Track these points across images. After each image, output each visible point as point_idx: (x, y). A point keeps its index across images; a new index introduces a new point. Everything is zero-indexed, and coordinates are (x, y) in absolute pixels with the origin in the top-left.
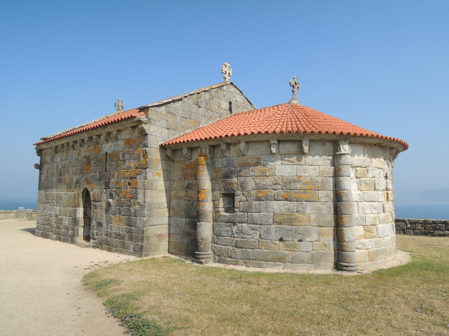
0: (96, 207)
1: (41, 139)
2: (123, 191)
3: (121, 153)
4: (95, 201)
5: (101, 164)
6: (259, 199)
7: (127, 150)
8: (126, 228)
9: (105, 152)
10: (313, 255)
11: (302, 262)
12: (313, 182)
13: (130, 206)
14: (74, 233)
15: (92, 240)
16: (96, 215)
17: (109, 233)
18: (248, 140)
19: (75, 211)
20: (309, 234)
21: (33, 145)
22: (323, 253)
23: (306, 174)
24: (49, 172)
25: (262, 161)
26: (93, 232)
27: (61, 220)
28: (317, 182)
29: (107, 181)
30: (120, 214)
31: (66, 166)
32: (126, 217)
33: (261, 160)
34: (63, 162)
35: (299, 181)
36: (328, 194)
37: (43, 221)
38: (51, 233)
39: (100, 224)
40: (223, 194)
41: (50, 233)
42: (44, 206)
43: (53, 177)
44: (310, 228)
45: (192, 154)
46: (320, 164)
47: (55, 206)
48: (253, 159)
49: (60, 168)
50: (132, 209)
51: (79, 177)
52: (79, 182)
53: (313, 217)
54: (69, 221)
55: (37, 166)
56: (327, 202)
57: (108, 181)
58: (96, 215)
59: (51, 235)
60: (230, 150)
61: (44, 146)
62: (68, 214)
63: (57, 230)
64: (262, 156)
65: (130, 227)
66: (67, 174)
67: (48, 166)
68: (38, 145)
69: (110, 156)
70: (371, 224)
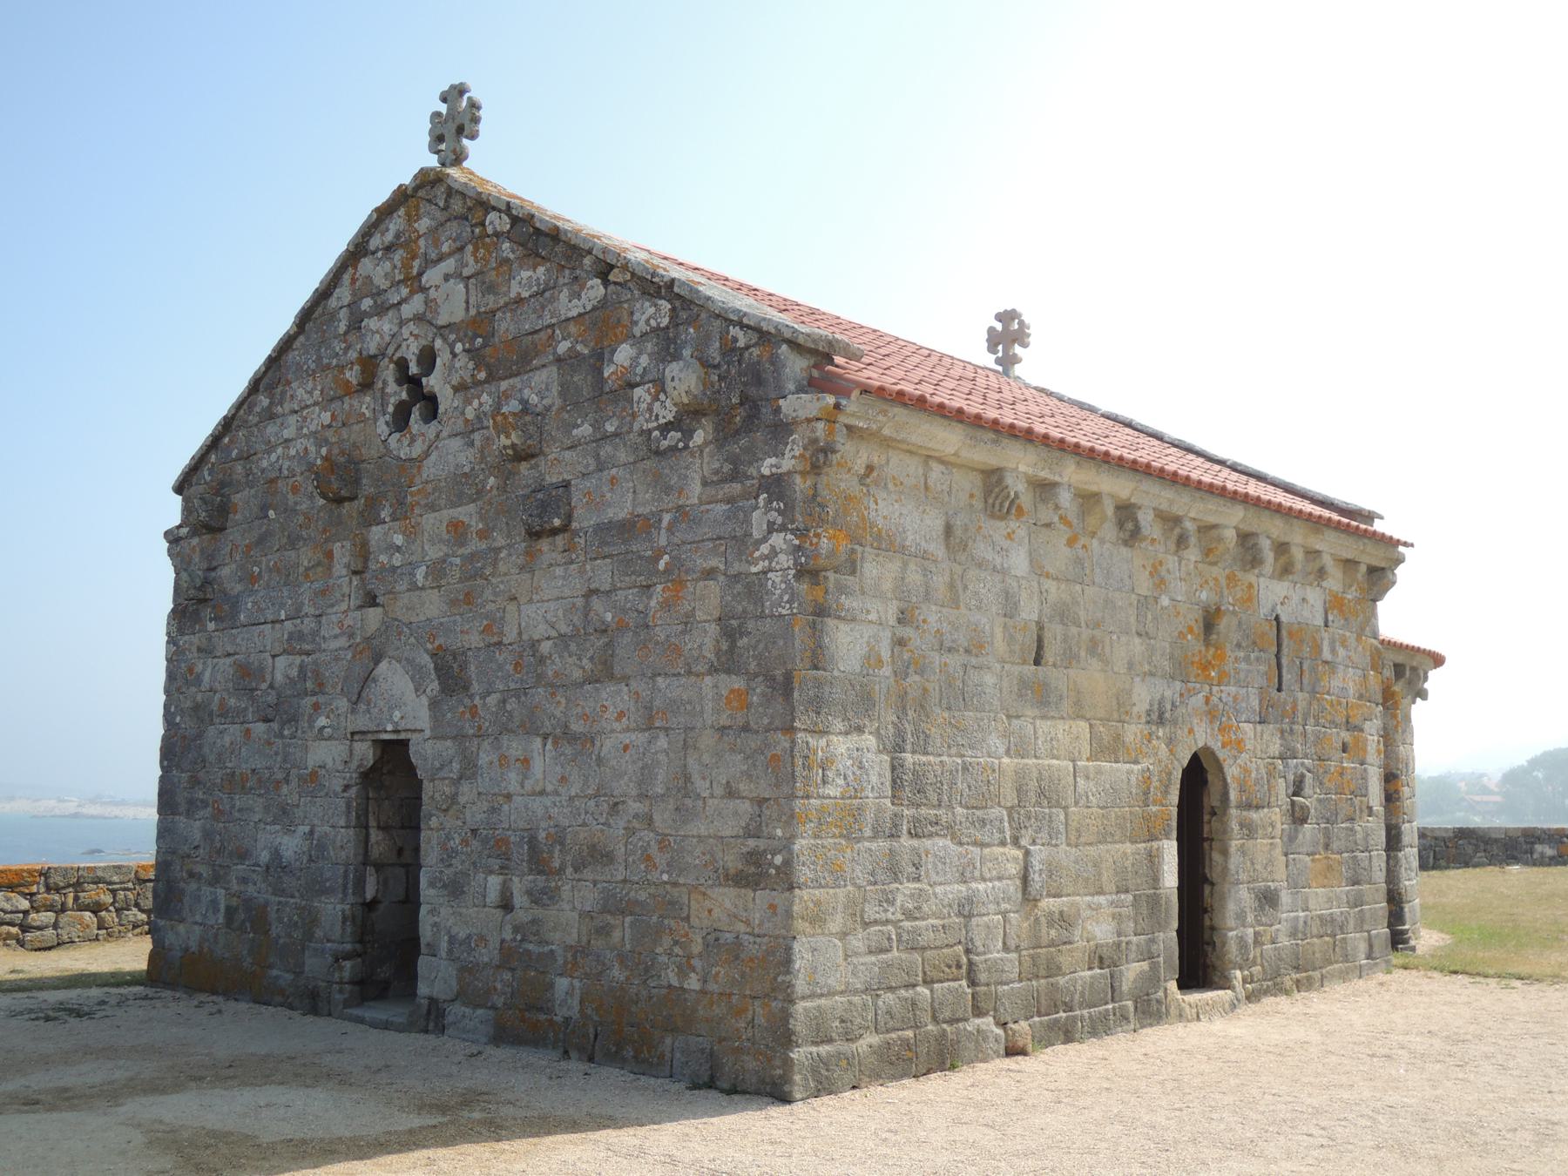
0: (1249, 830)
2: (1332, 770)
4: (1248, 806)
8: (1348, 891)
16: (1253, 864)
19: (1153, 859)
47: (1003, 843)
51: (1171, 691)
52: (1167, 715)
54: (1117, 917)
58: (1253, 864)
65: (1356, 887)
66: (1095, 664)
69: (1290, 634)
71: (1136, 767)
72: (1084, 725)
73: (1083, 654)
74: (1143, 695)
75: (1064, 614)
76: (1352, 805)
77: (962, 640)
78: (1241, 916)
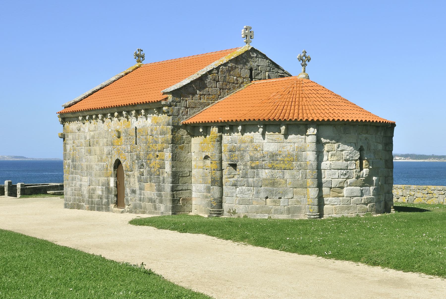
0: (129, 176)
3: (149, 129)
5: (131, 137)
7: (155, 127)
8: (157, 193)
9: (135, 127)
13: (159, 175)
14: (108, 201)
15: (127, 206)
16: (130, 183)
17: (142, 199)
18: (243, 124)
21: (57, 113)
22: (296, 207)
23: (285, 150)
24: (76, 142)
25: (254, 140)
26: (127, 199)
27: (94, 190)
28: (292, 155)
29: (138, 153)
30: (150, 181)
31: (96, 137)
32: (156, 184)
33: (253, 139)
34: (92, 133)
36: (301, 164)
37: (73, 192)
38: (82, 203)
39: (134, 192)
40: (229, 164)
41: (82, 203)
42: (73, 177)
43: (81, 147)
44: (287, 189)
45: (207, 131)
46: (295, 142)
48: (248, 137)
49: (88, 138)
50: (161, 177)
52: (110, 153)
53: (289, 181)
54: (102, 191)
56: (300, 170)
57: (139, 153)
59: (83, 206)
60: (233, 130)
62: (100, 185)
63: (90, 199)
64: (254, 136)
67: (74, 136)
70: (337, 186)
71: (105, 163)
72: (96, 156)
73: (96, 144)
74: (106, 150)
75: (93, 137)
76: (159, 171)
77: (79, 144)
78: (127, 195)
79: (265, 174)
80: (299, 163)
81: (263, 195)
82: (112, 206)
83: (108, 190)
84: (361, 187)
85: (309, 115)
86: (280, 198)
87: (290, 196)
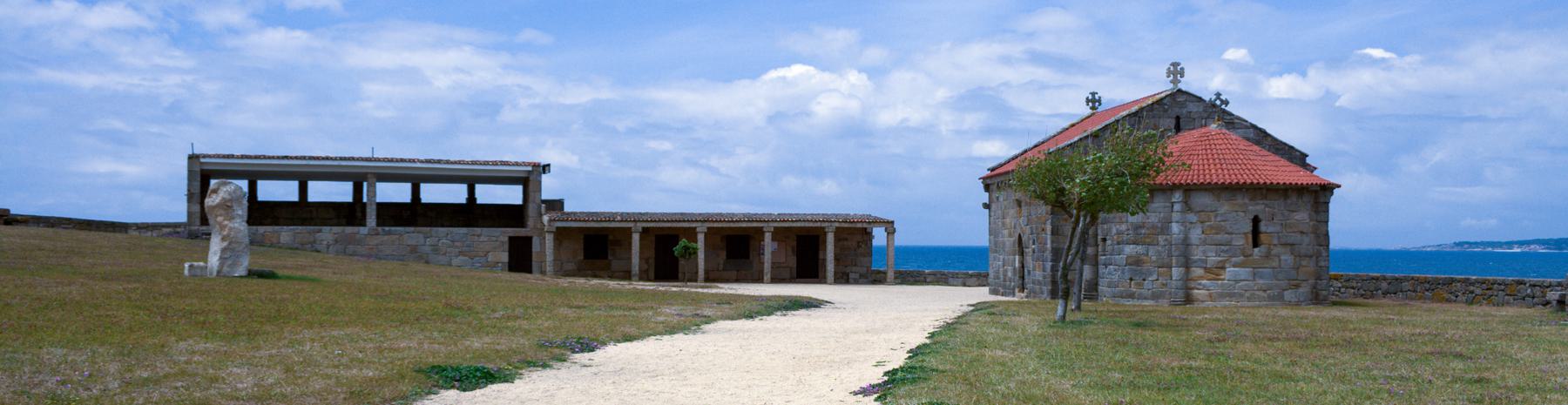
1: (988, 170)
6: (1118, 243)
10: (1153, 293)
11: (1146, 298)
12: (1154, 227)
20: (1151, 274)
28: (1157, 227)
35: (1144, 227)
55: (986, 206)
61: (989, 181)
68: (984, 179)
79: (1129, 249)
80: (1164, 237)
81: (1127, 276)
82: (1017, 290)
83: (1015, 269)
84: (1254, 268)
85: (1239, 177)
86: (1144, 280)
87: (1155, 277)
